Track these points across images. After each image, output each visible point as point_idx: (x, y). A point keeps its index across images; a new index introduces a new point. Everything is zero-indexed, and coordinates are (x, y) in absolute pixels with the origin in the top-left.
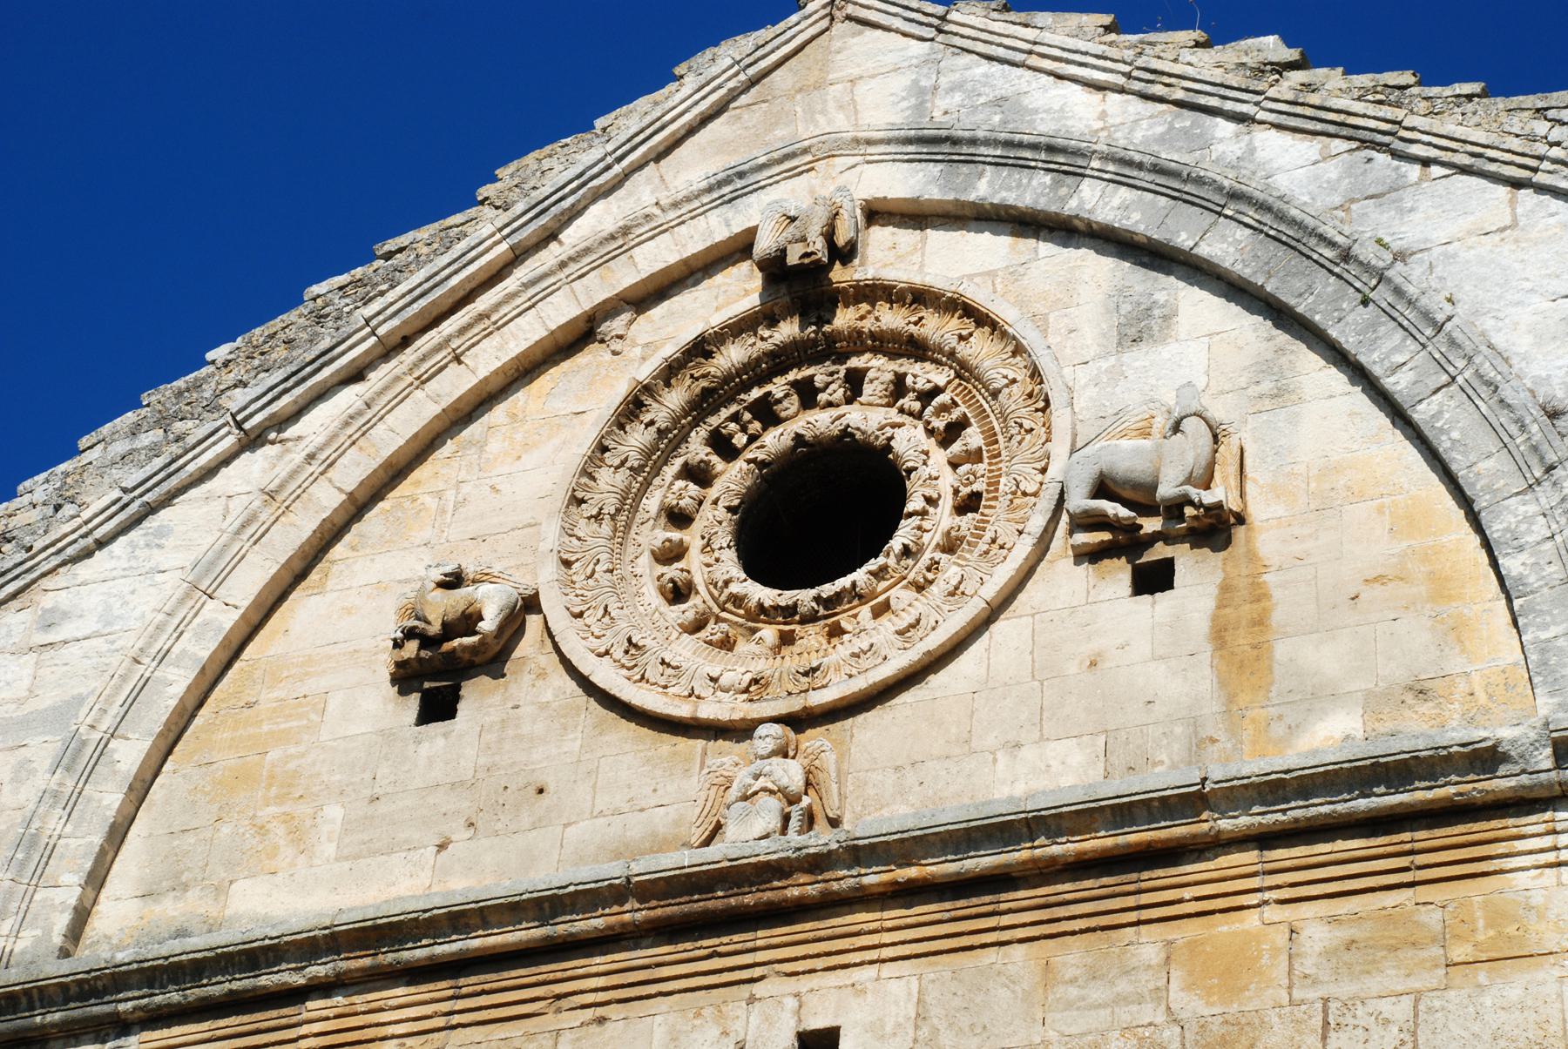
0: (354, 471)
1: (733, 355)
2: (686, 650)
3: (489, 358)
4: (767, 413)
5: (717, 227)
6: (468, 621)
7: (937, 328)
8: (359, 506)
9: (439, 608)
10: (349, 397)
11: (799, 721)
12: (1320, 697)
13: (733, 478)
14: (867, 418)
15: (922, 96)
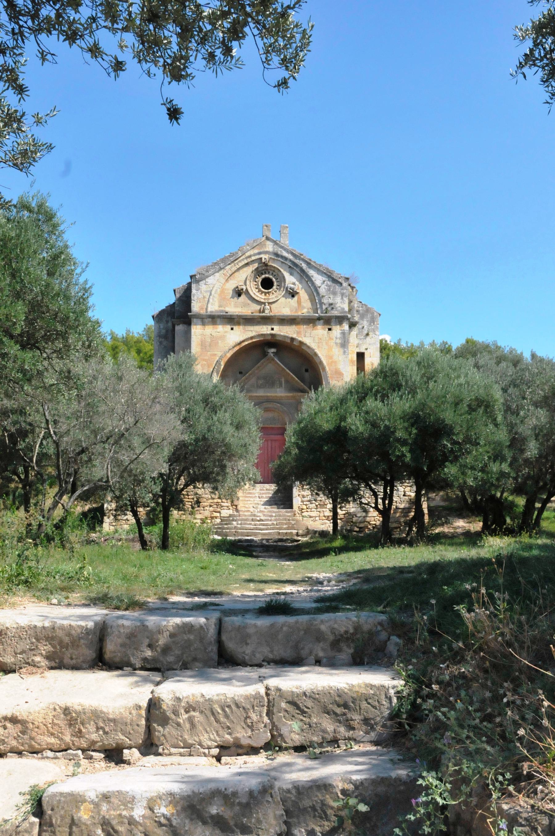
0: (230, 272)
1: (260, 269)
2: (258, 294)
3: (241, 264)
4: (262, 274)
5: (257, 257)
6: (242, 289)
7: (276, 271)
8: (231, 275)
9: (240, 288)
10: (229, 266)
11: (269, 303)
12: (304, 308)
13: (260, 280)
14: (271, 277)
15: (274, 248)
